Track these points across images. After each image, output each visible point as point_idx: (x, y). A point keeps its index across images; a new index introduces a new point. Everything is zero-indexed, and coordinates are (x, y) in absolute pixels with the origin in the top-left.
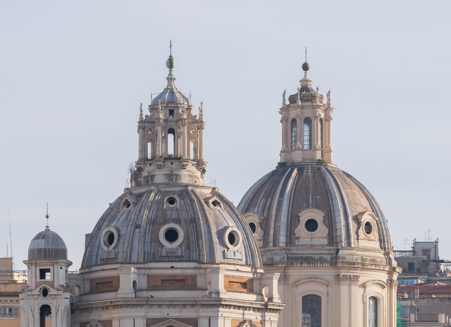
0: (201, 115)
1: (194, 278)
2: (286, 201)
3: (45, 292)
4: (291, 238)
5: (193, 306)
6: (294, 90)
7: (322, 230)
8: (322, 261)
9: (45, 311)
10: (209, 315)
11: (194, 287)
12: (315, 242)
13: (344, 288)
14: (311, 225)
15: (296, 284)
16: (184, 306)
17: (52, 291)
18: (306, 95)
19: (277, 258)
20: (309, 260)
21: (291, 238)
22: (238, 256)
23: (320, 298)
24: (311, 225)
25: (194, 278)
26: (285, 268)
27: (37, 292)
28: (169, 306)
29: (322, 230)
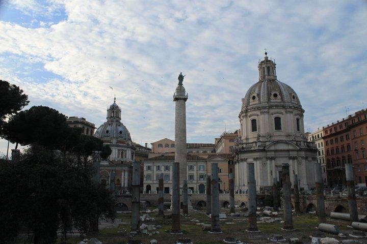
4: (269, 99)
6: (264, 59)
12: (278, 101)
13: (288, 115)
14: (275, 95)
21: (269, 99)
23: (280, 118)
26: (268, 109)
29: (279, 97)
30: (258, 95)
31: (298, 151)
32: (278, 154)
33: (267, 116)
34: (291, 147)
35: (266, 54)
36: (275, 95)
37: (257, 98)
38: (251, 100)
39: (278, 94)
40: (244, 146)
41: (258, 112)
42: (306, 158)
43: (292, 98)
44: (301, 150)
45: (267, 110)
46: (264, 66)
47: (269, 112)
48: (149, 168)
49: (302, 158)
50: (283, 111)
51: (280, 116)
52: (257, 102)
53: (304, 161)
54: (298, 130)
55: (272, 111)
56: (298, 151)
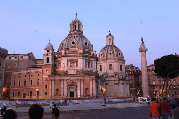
0: (82, 23)
1: (77, 51)
2: (106, 50)
3: (48, 55)
5: (77, 56)
7: (112, 54)
8: (112, 59)
9: (48, 59)
10: (80, 58)
11: (77, 53)
12: (112, 56)
15: (108, 63)
16: (75, 56)
17: (49, 54)
18: (110, 35)
19: (105, 59)
20: (110, 59)
22: (87, 47)
24: (110, 54)
25: (77, 51)
27: (46, 55)
28: (72, 56)
29: (112, 54)
30: (103, 54)
31: (119, 80)
33: (105, 64)
34: (115, 79)
35: (110, 32)
36: (110, 54)
37: (102, 55)
41: (102, 62)
42: (123, 84)
43: (119, 54)
44: (120, 80)
45: (105, 61)
46: (108, 38)
47: (106, 62)
50: (113, 61)
52: (103, 57)
53: (122, 86)
55: (108, 61)
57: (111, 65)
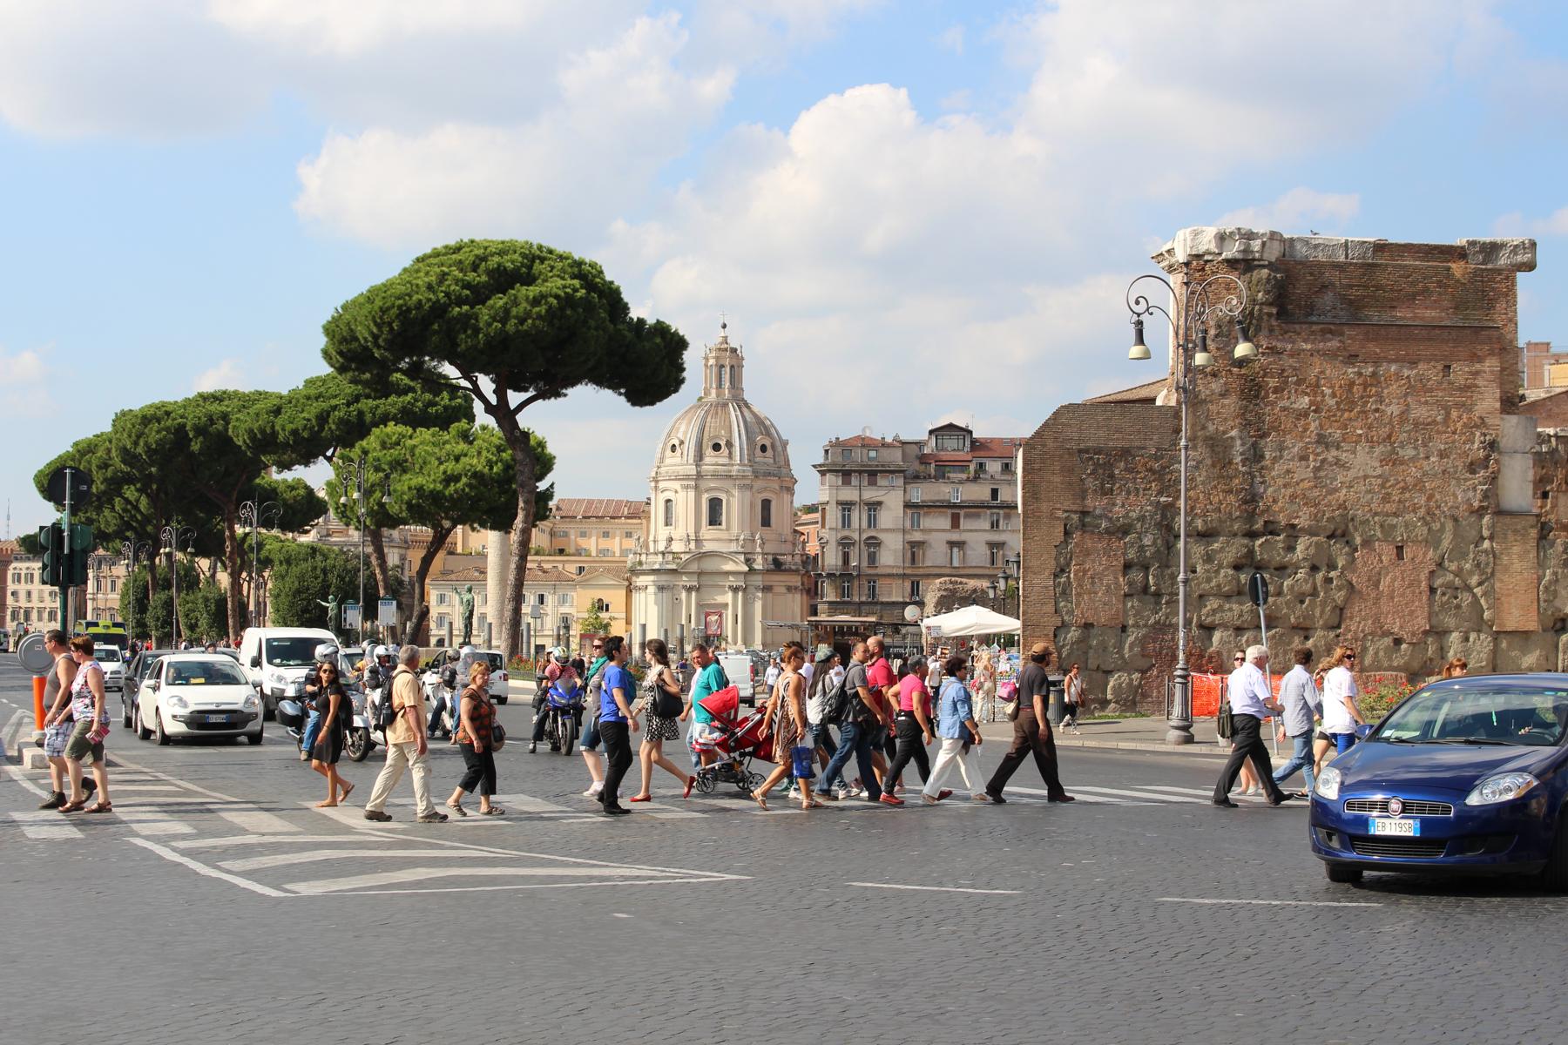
12: (721, 461)
30: (682, 443)
32: (705, 580)
36: (717, 447)
38: (668, 452)
39: (723, 443)
40: (643, 558)
41: (677, 485)
42: (767, 589)
48: (442, 599)
49: (757, 588)
50: (727, 484)
51: (723, 496)
54: (766, 522)
55: (704, 485)
56: (746, 574)
57: (715, 505)
